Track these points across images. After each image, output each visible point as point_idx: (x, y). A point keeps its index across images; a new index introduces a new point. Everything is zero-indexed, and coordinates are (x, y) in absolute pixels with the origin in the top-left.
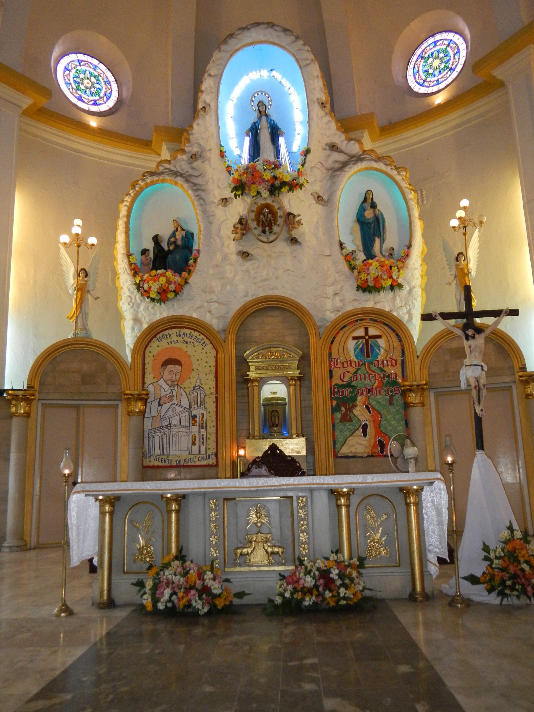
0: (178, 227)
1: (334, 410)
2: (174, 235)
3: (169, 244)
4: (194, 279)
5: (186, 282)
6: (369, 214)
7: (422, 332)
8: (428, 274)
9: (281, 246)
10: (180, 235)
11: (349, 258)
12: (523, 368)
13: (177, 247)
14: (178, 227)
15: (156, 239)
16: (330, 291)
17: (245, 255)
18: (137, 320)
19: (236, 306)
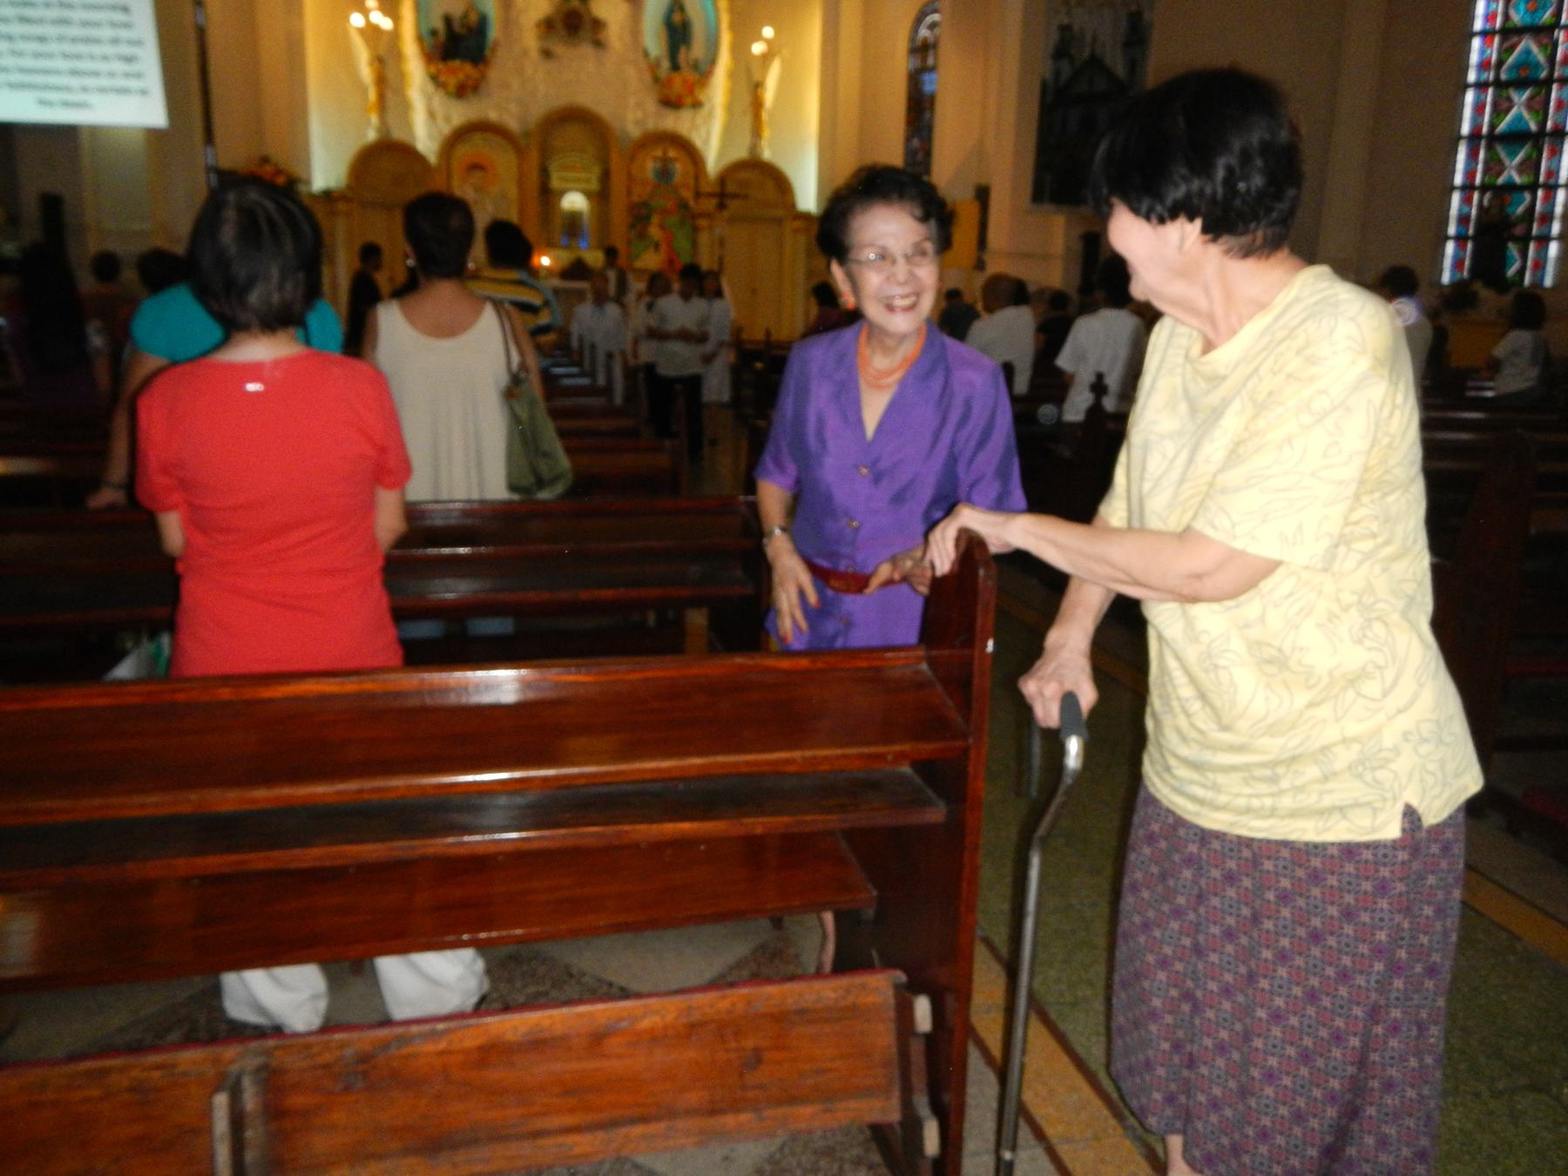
0: (471, 7)
1: (632, 226)
2: (465, 15)
3: (463, 26)
4: (494, 74)
5: (483, 77)
6: (677, 18)
7: (721, 154)
8: (733, 93)
9: (587, 49)
10: (473, 18)
11: (654, 67)
12: (793, 205)
13: (470, 29)
14: (471, 7)
15: (448, 20)
16: (632, 101)
17: (547, 54)
18: (431, 114)
19: (537, 111)
